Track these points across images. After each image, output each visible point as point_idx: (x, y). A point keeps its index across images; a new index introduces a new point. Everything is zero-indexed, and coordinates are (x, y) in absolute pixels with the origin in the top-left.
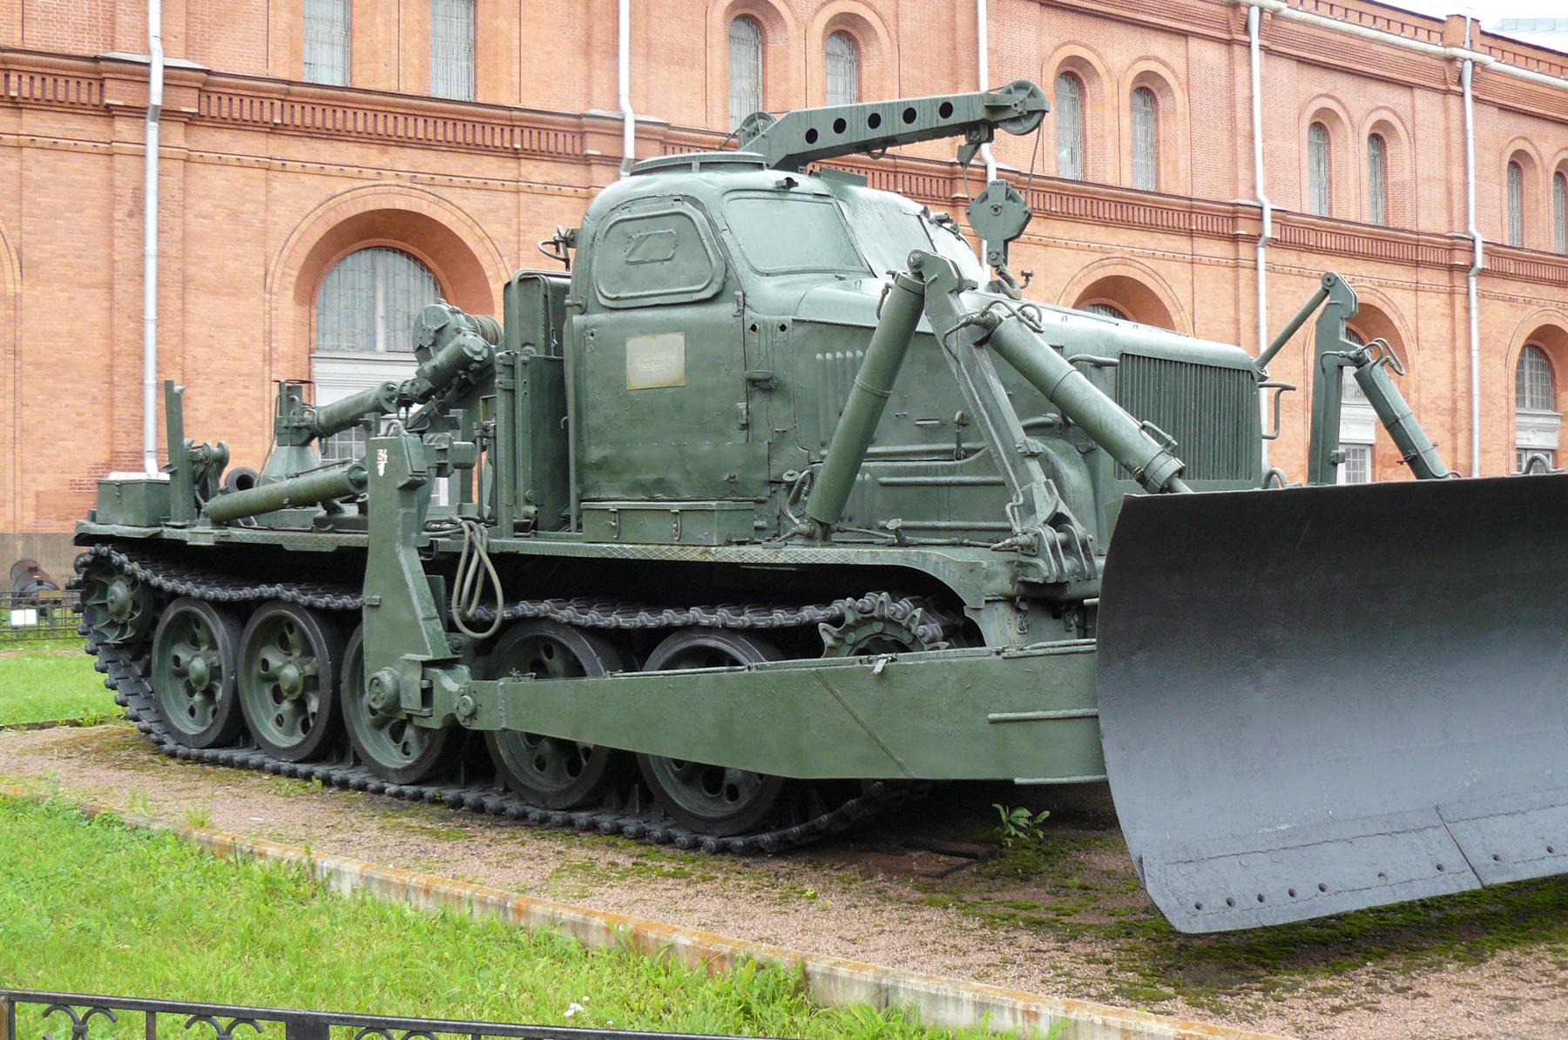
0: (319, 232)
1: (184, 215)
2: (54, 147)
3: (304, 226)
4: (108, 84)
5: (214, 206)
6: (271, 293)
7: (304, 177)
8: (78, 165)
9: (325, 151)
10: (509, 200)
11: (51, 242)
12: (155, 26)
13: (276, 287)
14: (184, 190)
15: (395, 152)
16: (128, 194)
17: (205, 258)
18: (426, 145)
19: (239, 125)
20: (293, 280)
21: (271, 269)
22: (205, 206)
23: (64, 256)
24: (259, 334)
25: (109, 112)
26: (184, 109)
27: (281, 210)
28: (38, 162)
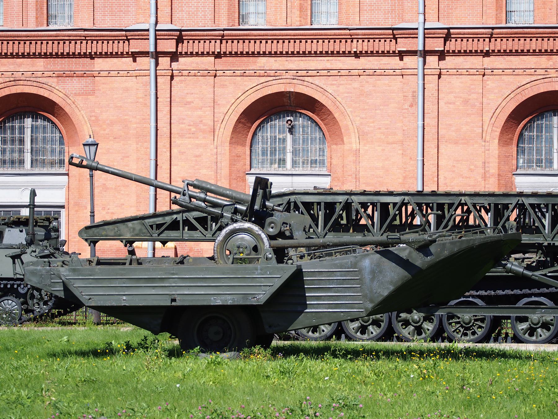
3: (504, 104)
4: (398, 40)
5: (455, 97)
6: (485, 142)
7: (504, 77)
8: (387, 82)
11: (373, 122)
13: (488, 138)
17: (450, 125)
20: (498, 134)
21: (485, 128)
23: (380, 129)
24: (480, 164)
26: (437, 49)
27: (492, 96)
28: (368, 82)
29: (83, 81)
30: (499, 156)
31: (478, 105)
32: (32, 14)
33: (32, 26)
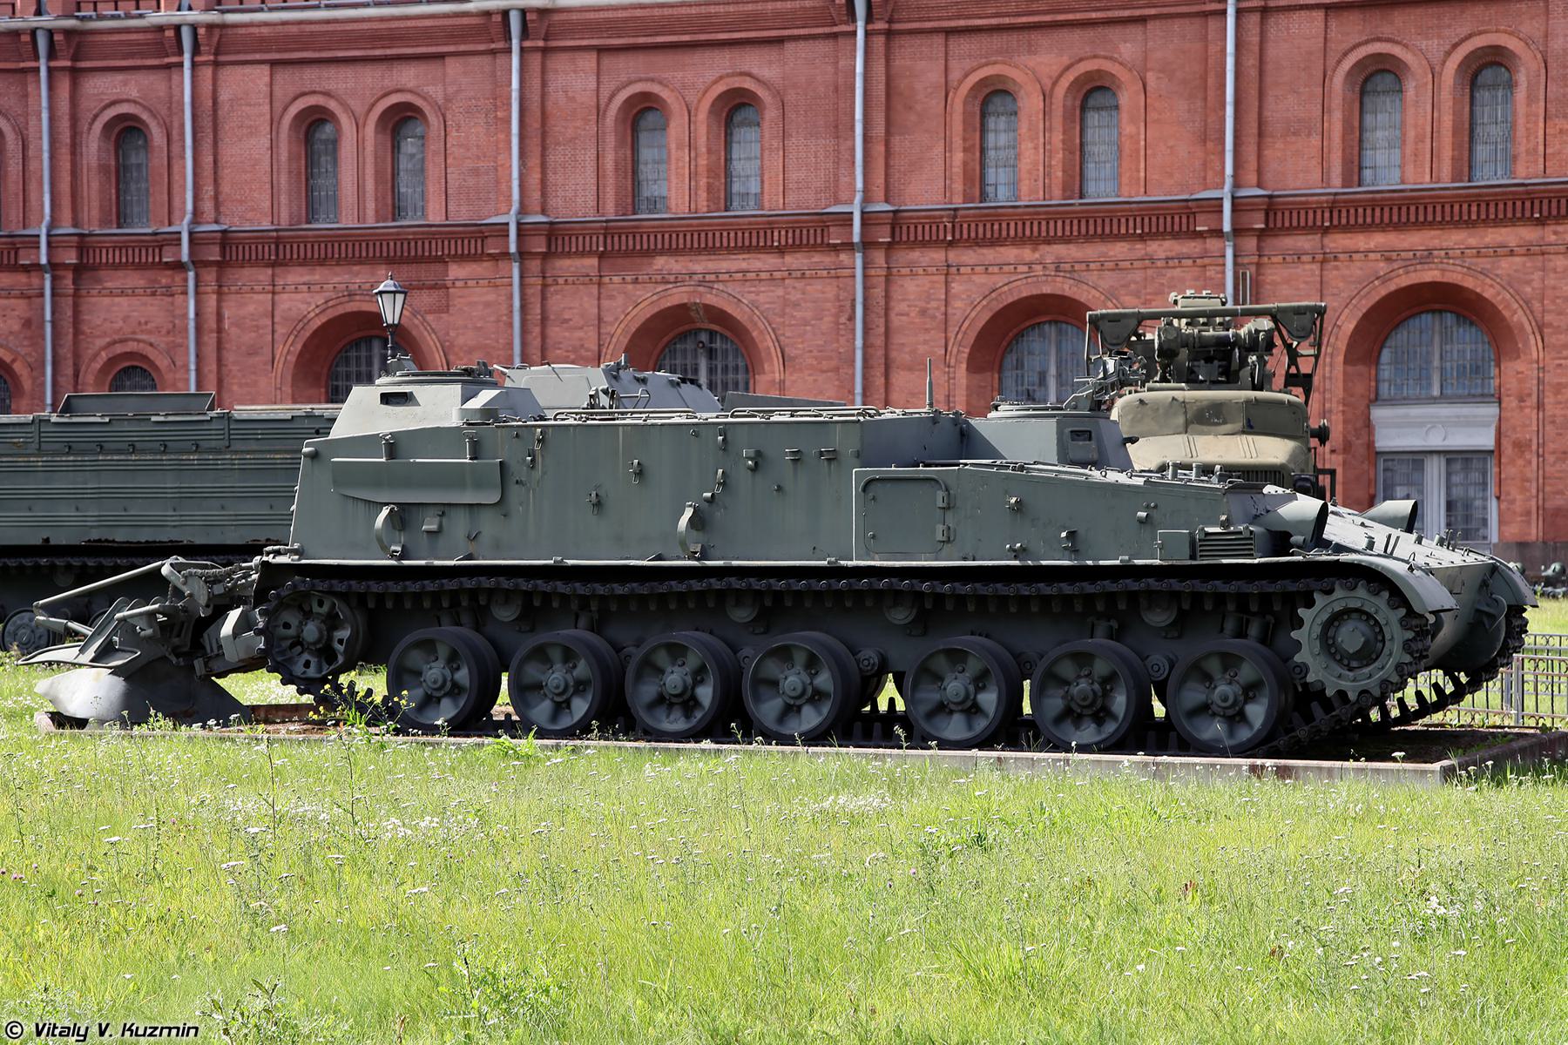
0: (986, 316)
1: (887, 315)
2: (803, 276)
3: (973, 314)
7: (974, 278)
9: (989, 254)
10: (1138, 276)
12: (859, 185)
13: (953, 362)
14: (887, 297)
15: (1044, 248)
16: (848, 304)
18: (1066, 240)
19: (924, 244)
22: (903, 307)
25: (835, 248)
29: (436, 294)
30: (968, 387)
31: (941, 317)
32: (371, 206)
33: (370, 223)
